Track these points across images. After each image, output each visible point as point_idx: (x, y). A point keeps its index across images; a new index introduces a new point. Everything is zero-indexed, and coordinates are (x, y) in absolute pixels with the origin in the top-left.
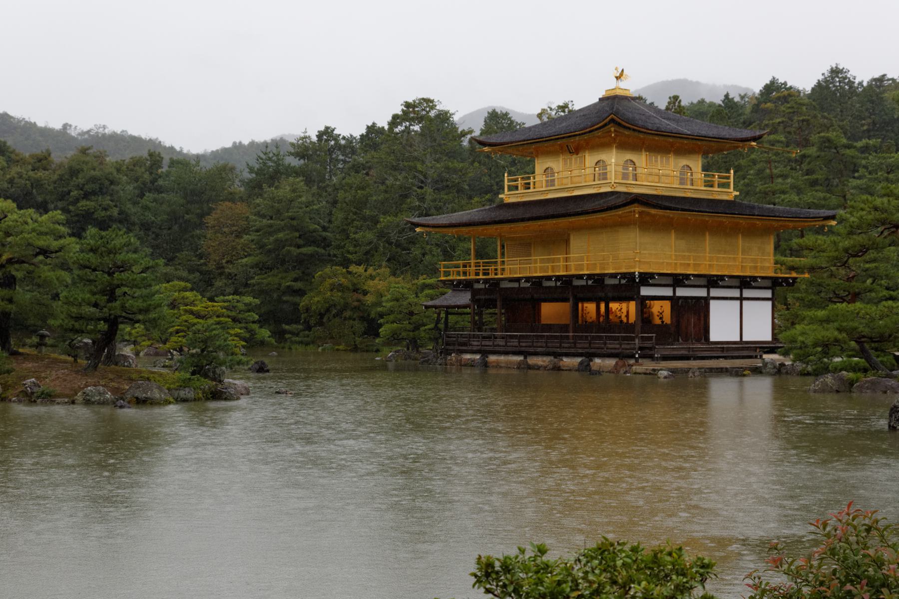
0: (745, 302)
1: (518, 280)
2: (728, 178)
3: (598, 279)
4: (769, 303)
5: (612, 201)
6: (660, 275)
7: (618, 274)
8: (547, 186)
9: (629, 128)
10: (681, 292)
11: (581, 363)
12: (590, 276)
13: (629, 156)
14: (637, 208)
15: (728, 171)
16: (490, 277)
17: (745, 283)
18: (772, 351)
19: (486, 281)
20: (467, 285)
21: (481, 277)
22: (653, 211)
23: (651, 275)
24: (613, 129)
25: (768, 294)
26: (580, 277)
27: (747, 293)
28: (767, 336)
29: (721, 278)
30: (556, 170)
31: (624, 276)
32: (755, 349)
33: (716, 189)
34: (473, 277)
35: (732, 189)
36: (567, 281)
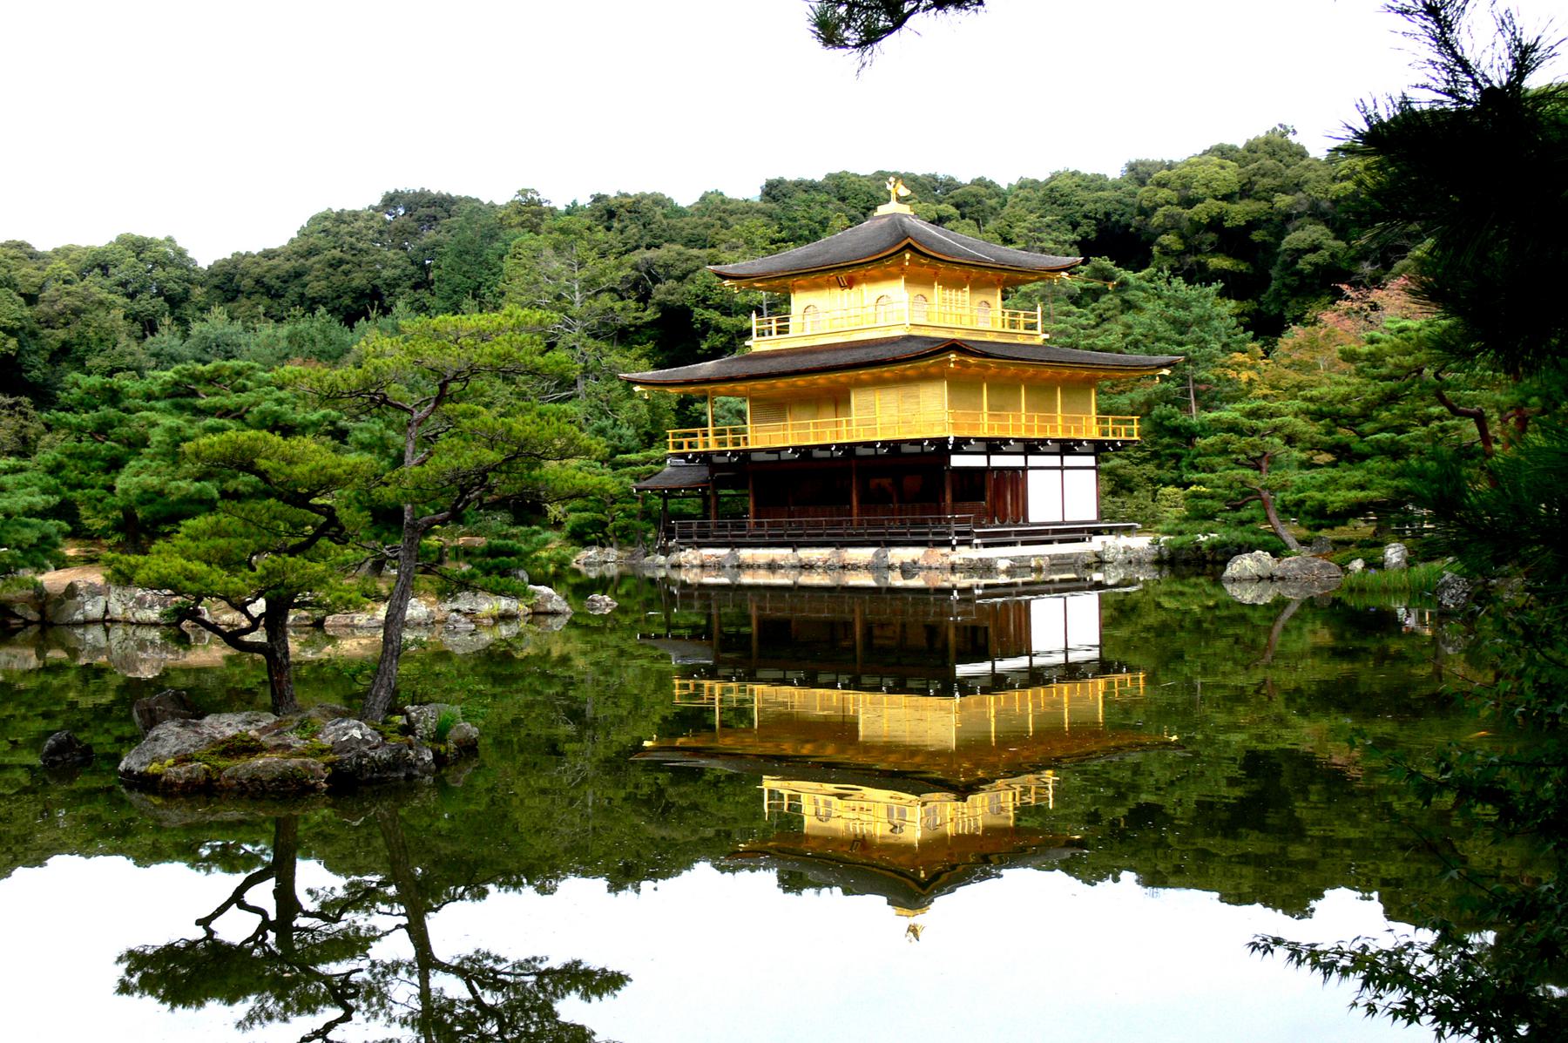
1: (777, 451)
2: (1035, 317)
3: (894, 446)
5: (914, 348)
6: (977, 439)
10: (998, 461)
11: (876, 555)
12: (885, 444)
13: (919, 290)
14: (953, 357)
15: (1034, 309)
16: (742, 447)
17: (1067, 447)
18: (1097, 532)
19: (734, 453)
20: (706, 458)
21: (730, 447)
22: (971, 360)
23: (966, 441)
24: (908, 256)
26: (871, 444)
27: (1070, 460)
29: (1043, 442)
31: (932, 441)
32: (1081, 530)
33: (1022, 330)
34: (713, 447)
35: (1039, 331)
36: (849, 448)
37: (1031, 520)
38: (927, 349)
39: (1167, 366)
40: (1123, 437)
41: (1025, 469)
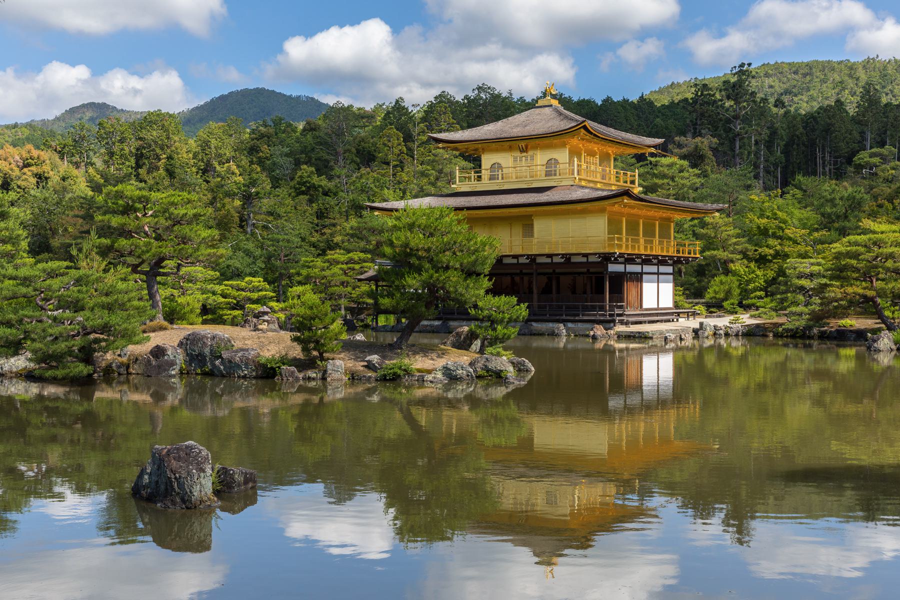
0: (660, 276)
2: (634, 176)
3: (567, 257)
4: (671, 277)
7: (595, 254)
8: (502, 178)
9: (591, 133)
10: (631, 268)
17: (662, 262)
25: (670, 269)
27: (663, 269)
28: (670, 304)
30: (503, 165)
36: (532, 258)
37: (645, 306)
38: (605, 193)
39: (718, 211)
40: (692, 255)
41: (642, 274)
